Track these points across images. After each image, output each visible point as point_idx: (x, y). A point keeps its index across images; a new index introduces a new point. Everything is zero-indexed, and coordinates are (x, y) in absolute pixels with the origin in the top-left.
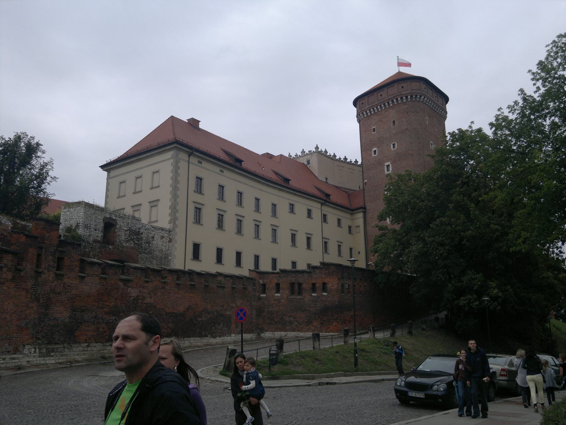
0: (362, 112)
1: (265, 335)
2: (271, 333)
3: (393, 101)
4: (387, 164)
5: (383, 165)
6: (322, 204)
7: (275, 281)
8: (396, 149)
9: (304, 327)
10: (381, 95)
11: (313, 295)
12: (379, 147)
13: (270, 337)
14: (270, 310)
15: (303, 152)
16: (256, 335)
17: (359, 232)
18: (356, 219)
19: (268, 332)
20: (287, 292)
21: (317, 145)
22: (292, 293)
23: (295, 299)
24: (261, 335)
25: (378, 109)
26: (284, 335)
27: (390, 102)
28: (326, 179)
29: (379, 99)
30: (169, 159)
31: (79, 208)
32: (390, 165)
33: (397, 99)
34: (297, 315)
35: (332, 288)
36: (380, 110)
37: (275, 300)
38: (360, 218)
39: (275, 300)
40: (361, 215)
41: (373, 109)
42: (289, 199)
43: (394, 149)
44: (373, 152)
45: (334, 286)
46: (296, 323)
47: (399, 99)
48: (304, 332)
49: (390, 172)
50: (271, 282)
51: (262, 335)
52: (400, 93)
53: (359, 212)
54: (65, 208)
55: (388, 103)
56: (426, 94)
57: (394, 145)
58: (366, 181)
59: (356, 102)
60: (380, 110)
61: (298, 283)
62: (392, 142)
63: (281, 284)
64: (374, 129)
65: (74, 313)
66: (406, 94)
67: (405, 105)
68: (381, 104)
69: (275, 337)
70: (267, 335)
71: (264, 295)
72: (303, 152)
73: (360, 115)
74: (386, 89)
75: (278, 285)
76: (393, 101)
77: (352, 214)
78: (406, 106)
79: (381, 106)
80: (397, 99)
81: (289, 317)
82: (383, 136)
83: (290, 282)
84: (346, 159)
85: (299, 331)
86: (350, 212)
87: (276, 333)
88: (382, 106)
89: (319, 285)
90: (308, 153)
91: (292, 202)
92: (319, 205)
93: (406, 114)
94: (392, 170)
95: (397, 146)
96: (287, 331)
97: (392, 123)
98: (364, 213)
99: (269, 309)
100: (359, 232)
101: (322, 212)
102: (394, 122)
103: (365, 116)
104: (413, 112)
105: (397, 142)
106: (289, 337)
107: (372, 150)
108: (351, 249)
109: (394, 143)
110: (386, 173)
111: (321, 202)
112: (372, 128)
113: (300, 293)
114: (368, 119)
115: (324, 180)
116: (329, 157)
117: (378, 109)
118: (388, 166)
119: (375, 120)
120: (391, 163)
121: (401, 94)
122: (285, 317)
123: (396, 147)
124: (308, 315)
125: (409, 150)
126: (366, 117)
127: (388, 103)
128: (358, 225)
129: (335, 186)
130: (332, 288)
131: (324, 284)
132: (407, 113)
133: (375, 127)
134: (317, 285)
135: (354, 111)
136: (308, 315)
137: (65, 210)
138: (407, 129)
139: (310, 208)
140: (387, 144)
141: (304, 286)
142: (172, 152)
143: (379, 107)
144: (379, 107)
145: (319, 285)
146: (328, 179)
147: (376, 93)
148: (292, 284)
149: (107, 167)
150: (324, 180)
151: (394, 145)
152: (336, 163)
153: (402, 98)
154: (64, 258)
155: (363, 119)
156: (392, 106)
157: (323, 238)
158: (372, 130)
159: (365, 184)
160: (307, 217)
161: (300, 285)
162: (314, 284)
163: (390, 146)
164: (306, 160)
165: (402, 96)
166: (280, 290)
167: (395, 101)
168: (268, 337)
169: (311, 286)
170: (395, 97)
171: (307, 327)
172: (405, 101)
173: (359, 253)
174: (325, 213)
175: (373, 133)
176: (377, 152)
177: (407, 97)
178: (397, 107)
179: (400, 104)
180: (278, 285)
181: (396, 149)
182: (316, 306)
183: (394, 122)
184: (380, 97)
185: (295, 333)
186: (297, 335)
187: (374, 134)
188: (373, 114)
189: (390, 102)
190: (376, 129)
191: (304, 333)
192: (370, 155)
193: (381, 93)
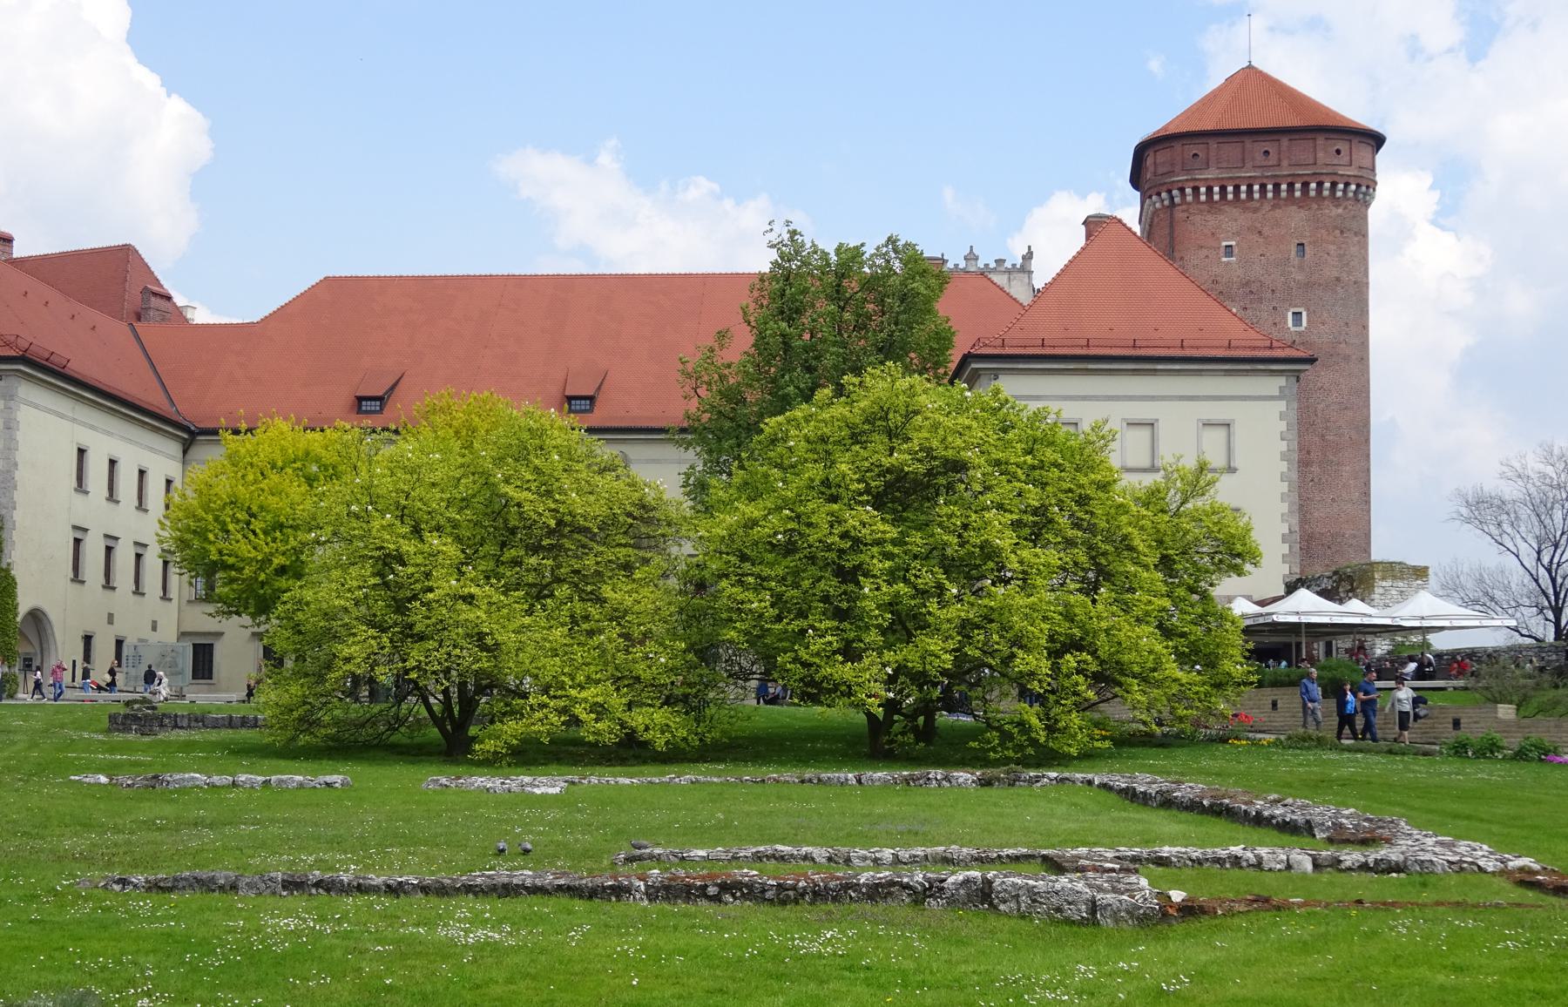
0: (1192, 184)
3: (1306, 185)
15: (971, 257)
21: (1029, 247)
27: (1298, 186)
30: (1272, 398)
31: (1419, 582)
33: (1320, 184)
36: (1256, 196)
43: (1297, 329)
52: (1329, 170)
54: (1383, 579)
55: (1291, 186)
57: (1297, 315)
66: (1349, 176)
67: (1337, 206)
68: (1265, 181)
72: (971, 257)
73: (1182, 190)
74: (1285, 142)
76: (1306, 185)
78: (1340, 211)
80: (1320, 184)
82: (1262, 279)
88: (1270, 187)
90: (993, 265)
93: (1338, 232)
95: (1308, 321)
97: (1294, 249)
103: (1203, 198)
104: (1356, 234)
105: (1308, 310)
109: (1296, 310)
112: (1224, 244)
119: (1236, 220)
121: (1335, 174)
126: (1203, 203)
127: (1291, 186)
132: (1342, 232)
133: (1233, 243)
137: (1384, 584)
138: (1338, 279)
142: (1281, 381)
143: (1256, 187)
151: (1297, 315)
153: (1334, 185)
155: (1189, 204)
156: (1298, 199)
158: (1223, 250)
163: (1285, 318)
165: (1336, 179)
175: (1224, 259)
177: (1347, 185)
178: (1315, 206)
181: (1303, 328)
184: (1259, 157)
187: (1228, 262)
188: (1230, 201)
189: (1298, 186)
190: (1236, 251)
193: (1267, 146)
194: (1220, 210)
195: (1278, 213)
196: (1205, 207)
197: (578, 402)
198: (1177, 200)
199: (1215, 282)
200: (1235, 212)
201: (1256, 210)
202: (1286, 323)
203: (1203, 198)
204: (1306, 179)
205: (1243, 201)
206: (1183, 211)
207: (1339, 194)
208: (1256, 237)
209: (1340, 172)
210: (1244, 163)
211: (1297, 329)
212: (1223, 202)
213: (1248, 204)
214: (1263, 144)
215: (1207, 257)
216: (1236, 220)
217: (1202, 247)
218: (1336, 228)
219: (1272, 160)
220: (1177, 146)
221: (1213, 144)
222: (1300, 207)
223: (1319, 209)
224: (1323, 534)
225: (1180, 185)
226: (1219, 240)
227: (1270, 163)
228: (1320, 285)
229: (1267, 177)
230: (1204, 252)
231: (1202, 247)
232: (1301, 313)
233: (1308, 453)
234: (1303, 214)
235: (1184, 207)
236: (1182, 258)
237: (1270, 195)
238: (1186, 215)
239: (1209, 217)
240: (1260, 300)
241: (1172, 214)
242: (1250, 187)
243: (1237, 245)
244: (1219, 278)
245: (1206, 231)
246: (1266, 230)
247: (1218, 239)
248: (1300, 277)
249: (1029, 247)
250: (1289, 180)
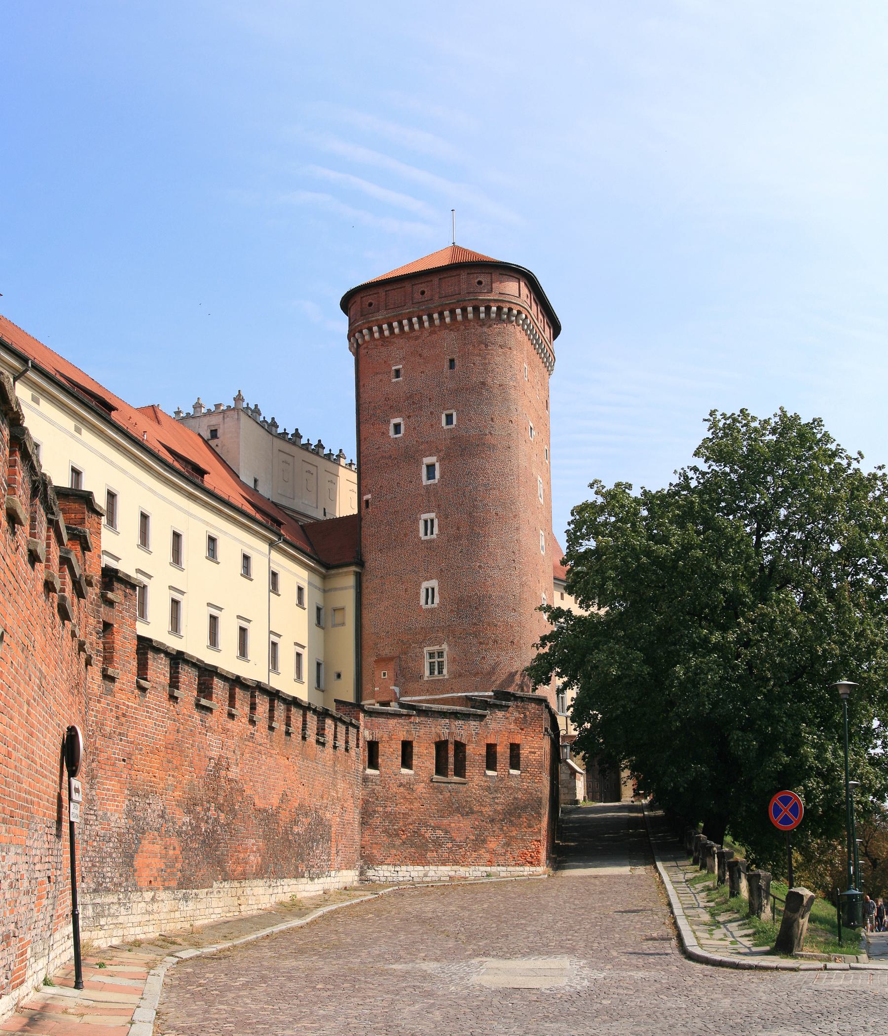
0: (366, 326)
1: (377, 874)
2: (391, 868)
4: (428, 460)
5: (419, 463)
6: (272, 544)
7: (403, 735)
8: (453, 426)
9: (468, 853)
10: (423, 293)
11: (490, 773)
12: (409, 417)
13: (390, 879)
14: (389, 809)
16: (357, 873)
17: (343, 624)
18: (336, 589)
19: (385, 867)
20: (431, 764)
22: (441, 769)
23: (448, 783)
24: (367, 874)
26: (421, 874)
28: (256, 481)
29: (415, 301)
32: (437, 466)
33: (464, 310)
34: (453, 825)
35: (531, 757)
36: (416, 326)
37: (401, 785)
38: (345, 588)
39: (401, 785)
40: (349, 581)
42: (207, 524)
44: (392, 428)
45: (535, 753)
46: (450, 845)
47: (470, 309)
48: (467, 866)
49: (436, 481)
50: (391, 739)
51: (370, 873)
53: (346, 574)
55: (441, 314)
56: (529, 309)
57: (449, 418)
58: (369, 496)
59: (348, 302)
60: (416, 326)
61: (456, 741)
62: (444, 409)
63: (415, 744)
65: (133, 799)
69: (401, 879)
70: (381, 873)
71: (377, 772)
73: (361, 332)
74: (436, 280)
75: (407, 747)
77: (324, 578)
80: (464, 310)
81: (434, 828)
83: (438, 740)
84: (297, 435)
85: (456, 863)
86: (323, 571)
87: (404, 868)
89: (503, 752)
91: (214, 534)
92: (264, 547)
94: (442, 477)
95: (458, 419)
96: (428, 863)
97: (447, 364)
98: (359, 577)
99: (386, 807)
100: (343, 624)
101: (271, 565)
102: (452, 361)
103: (377, 335)
106: (434, 879)
107: (389, 421)
108: (319, 665)
109: (448, 412)
110: (425, 482)
111: (270, 539)
112: (394, 368)
113: (460, 771)
114: (382, 345)
115: (252, 485)
116: (262, 424)
118: (431, 468)
119: (402, 348)
120: (440, 460)
122: (423, 830)
123: (455, 422)
124: (477, 823)
125: (486, 435)
128: (339, 605)
129: (272, 502)
130: (531, 757)
131: (515, 749)
134: (499, 749)
135: (342, 323)
136: (477, 823)
139: (248, 552)
140: (432, 413)
141: (470, 750)
143: (415, 320)
144: (415, 320)
145: (503, 752)
146: (260, 483)
147: (408, 285)
148: (441, 747)
150: (252, 485)
151: (449, 418)
152: (279, 443)
153: (476, 309)
154: (112, 625)
157: (271, 632)
158: (393, 374)
159: (363, 505)
160: (242, 575)
161: (460, 747)
162: (491, 749)
163: (440, 419)
164: (206, 428)
166: (414, 757)
167: (458, 311)
168: (383, 879)
169: (484, 752)
171: (474, 855)
172: (482, 316)
173: (339, 676)
174: (275, 568)
175: (394, 380)
176: (402, 427)
180: (407, 747)
181: (453, 426)
182: (496, 801)
183: (452, 361)
184: (418, 296)
185: (448, 868)
186: (452, 874)
190: (402, 372)
191: (467, 869)
192: (385, 434)
193: (422, 287)
195: (435, 337)
198: (360, 341)
199: (387, 399)
200: (401, 342)
201: (417, 338)
202: (440, 423)
207: (482, 316)
211: (450, 427)
212: (393, 336)
214: (420, 285)
215: (381, 380)
216: (402, 348)
217: (377, 373)
218: (481, 342)
221: (382, 292)
223: (466, 329)
224: (470, 597)
226: (390, 366)
227: (426, 299)
228: (467, 389)
229: (423, 310)
230: (380, 376)
231: (377, 373)
232: (452, 415)
233: (458, 529)
234: (453, 335)
235: (365, 345)
237: (426, 324)
238: (366, 351)
240: (421, 408)
242: (410, 321)
246: (425, 353)
248: (451, 385)
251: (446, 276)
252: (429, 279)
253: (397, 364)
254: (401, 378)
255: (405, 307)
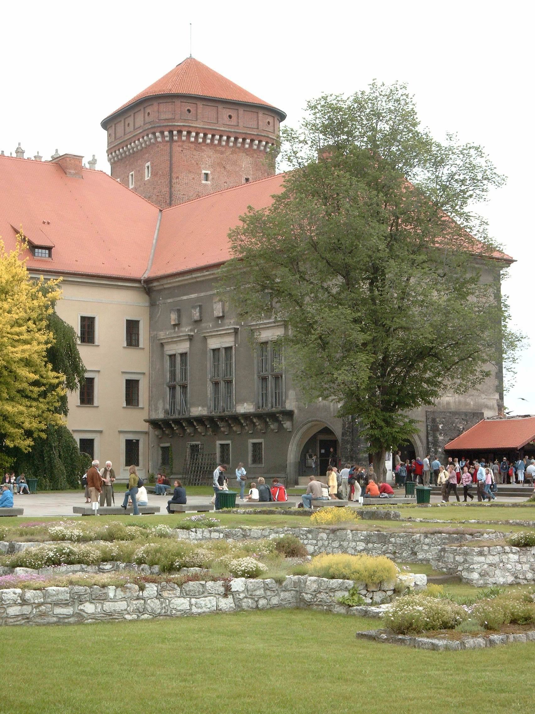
0: (187, 129)
21: (94, 156)
25: (220, 140)
41: (213, 136)
64: (206, 174)
79: (228, 138)
103: (192, 139)
112: (204, 172)
117: (220, 140)
119: (210, 157)
121: (268, 137)
126: (192, 142)
133: (209, 172)
147: (220, 107)
149: (106, 124)
155: (184, 141)
158: (203, 176)
170: (258, 135)
175: (204, 182)
179: (261, 151)
188: (208, 144)
190: (210, 177)
194: (201, 149)
196: (192, 145)
197: (40, 250)
201: (222, 153)
203: (192, 139)
204: (253, 137)
205: (215, 145)
206: (179, 146)
208: (222, 170)
209: (270, 136)
210: (218, 121)
212: (204, 144)
213: (218, 148)
219: (233, 122)
220: (178, 102)
221: (200, 104)
222: (247, 155)
225: (179, 129)
227: (232, 124)
231: (190, 172)
235: (180, 143)
236: (177, 178)
238: (181, 149)
239: (195, 153)
241: (171, 148)
243: (211, 173)
244: (200, 194)
245: (193, 162)
246: (228, 167)
247: (200, 167)
249: (94, 156)
250: (244, 136)
251: (248, 110)
252: (236, 108)
253: (206, 168)
254: (209, 182)
255: (217, 125)
